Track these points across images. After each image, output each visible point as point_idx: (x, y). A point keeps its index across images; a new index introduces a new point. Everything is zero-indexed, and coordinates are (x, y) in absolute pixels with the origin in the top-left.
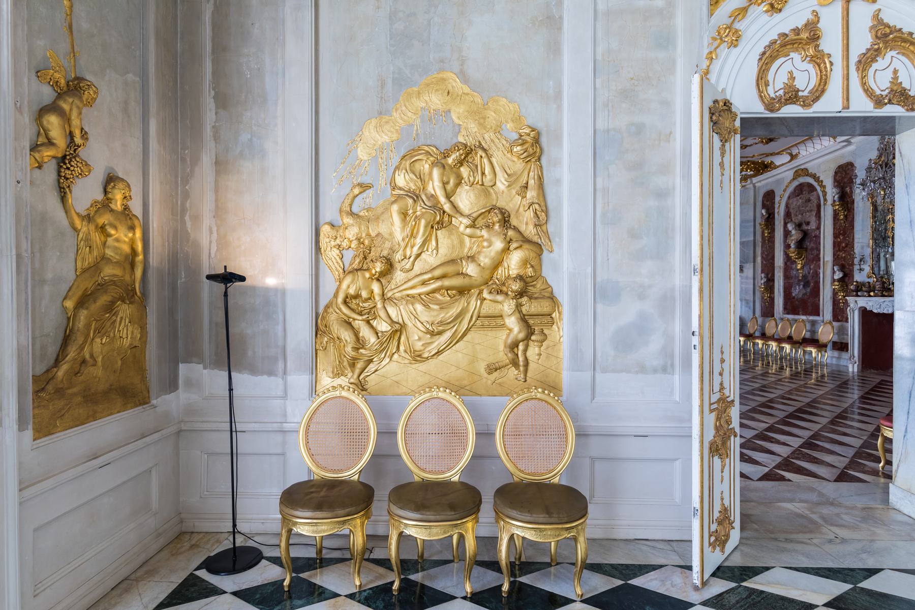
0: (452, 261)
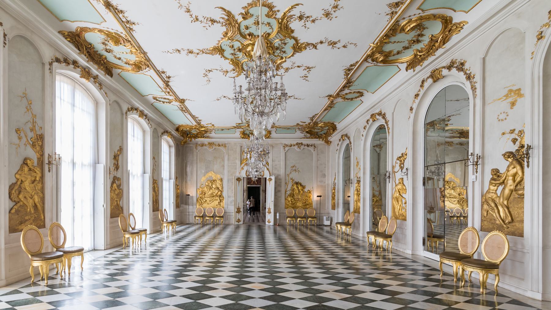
0: (212, 193)
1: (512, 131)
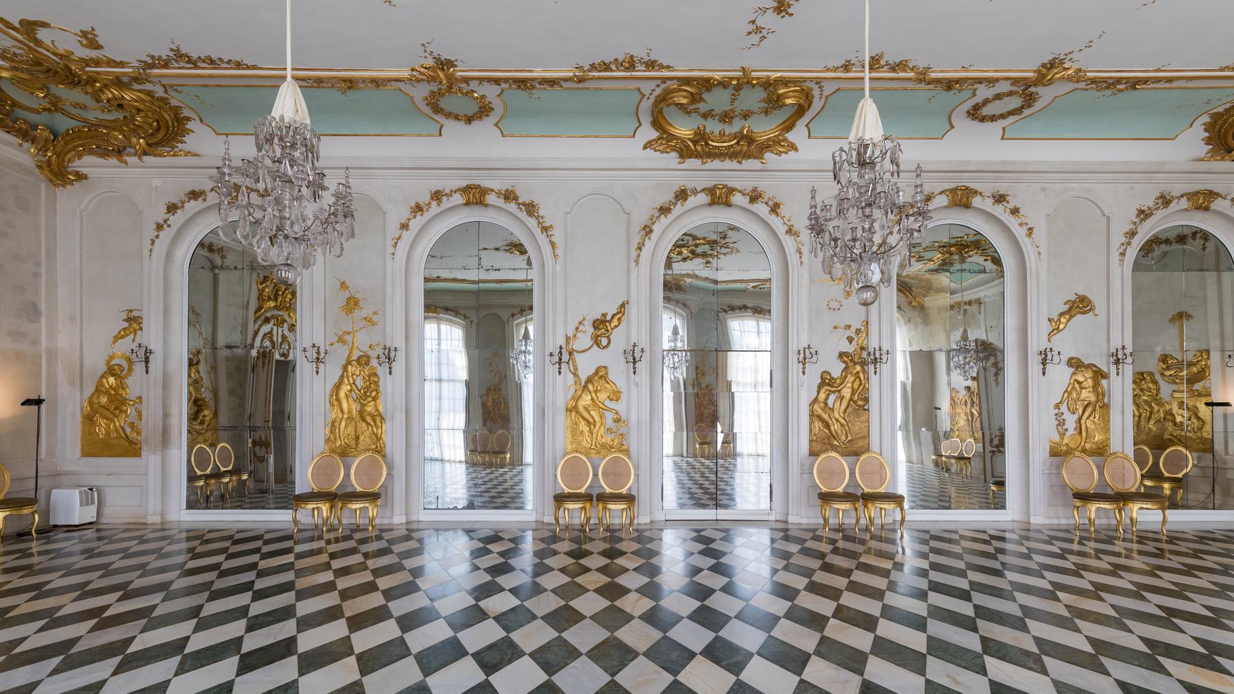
1: (848, 327)
